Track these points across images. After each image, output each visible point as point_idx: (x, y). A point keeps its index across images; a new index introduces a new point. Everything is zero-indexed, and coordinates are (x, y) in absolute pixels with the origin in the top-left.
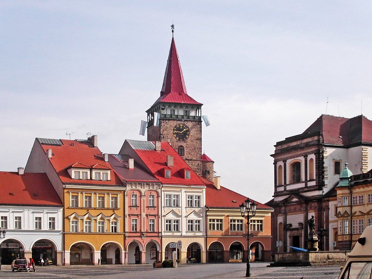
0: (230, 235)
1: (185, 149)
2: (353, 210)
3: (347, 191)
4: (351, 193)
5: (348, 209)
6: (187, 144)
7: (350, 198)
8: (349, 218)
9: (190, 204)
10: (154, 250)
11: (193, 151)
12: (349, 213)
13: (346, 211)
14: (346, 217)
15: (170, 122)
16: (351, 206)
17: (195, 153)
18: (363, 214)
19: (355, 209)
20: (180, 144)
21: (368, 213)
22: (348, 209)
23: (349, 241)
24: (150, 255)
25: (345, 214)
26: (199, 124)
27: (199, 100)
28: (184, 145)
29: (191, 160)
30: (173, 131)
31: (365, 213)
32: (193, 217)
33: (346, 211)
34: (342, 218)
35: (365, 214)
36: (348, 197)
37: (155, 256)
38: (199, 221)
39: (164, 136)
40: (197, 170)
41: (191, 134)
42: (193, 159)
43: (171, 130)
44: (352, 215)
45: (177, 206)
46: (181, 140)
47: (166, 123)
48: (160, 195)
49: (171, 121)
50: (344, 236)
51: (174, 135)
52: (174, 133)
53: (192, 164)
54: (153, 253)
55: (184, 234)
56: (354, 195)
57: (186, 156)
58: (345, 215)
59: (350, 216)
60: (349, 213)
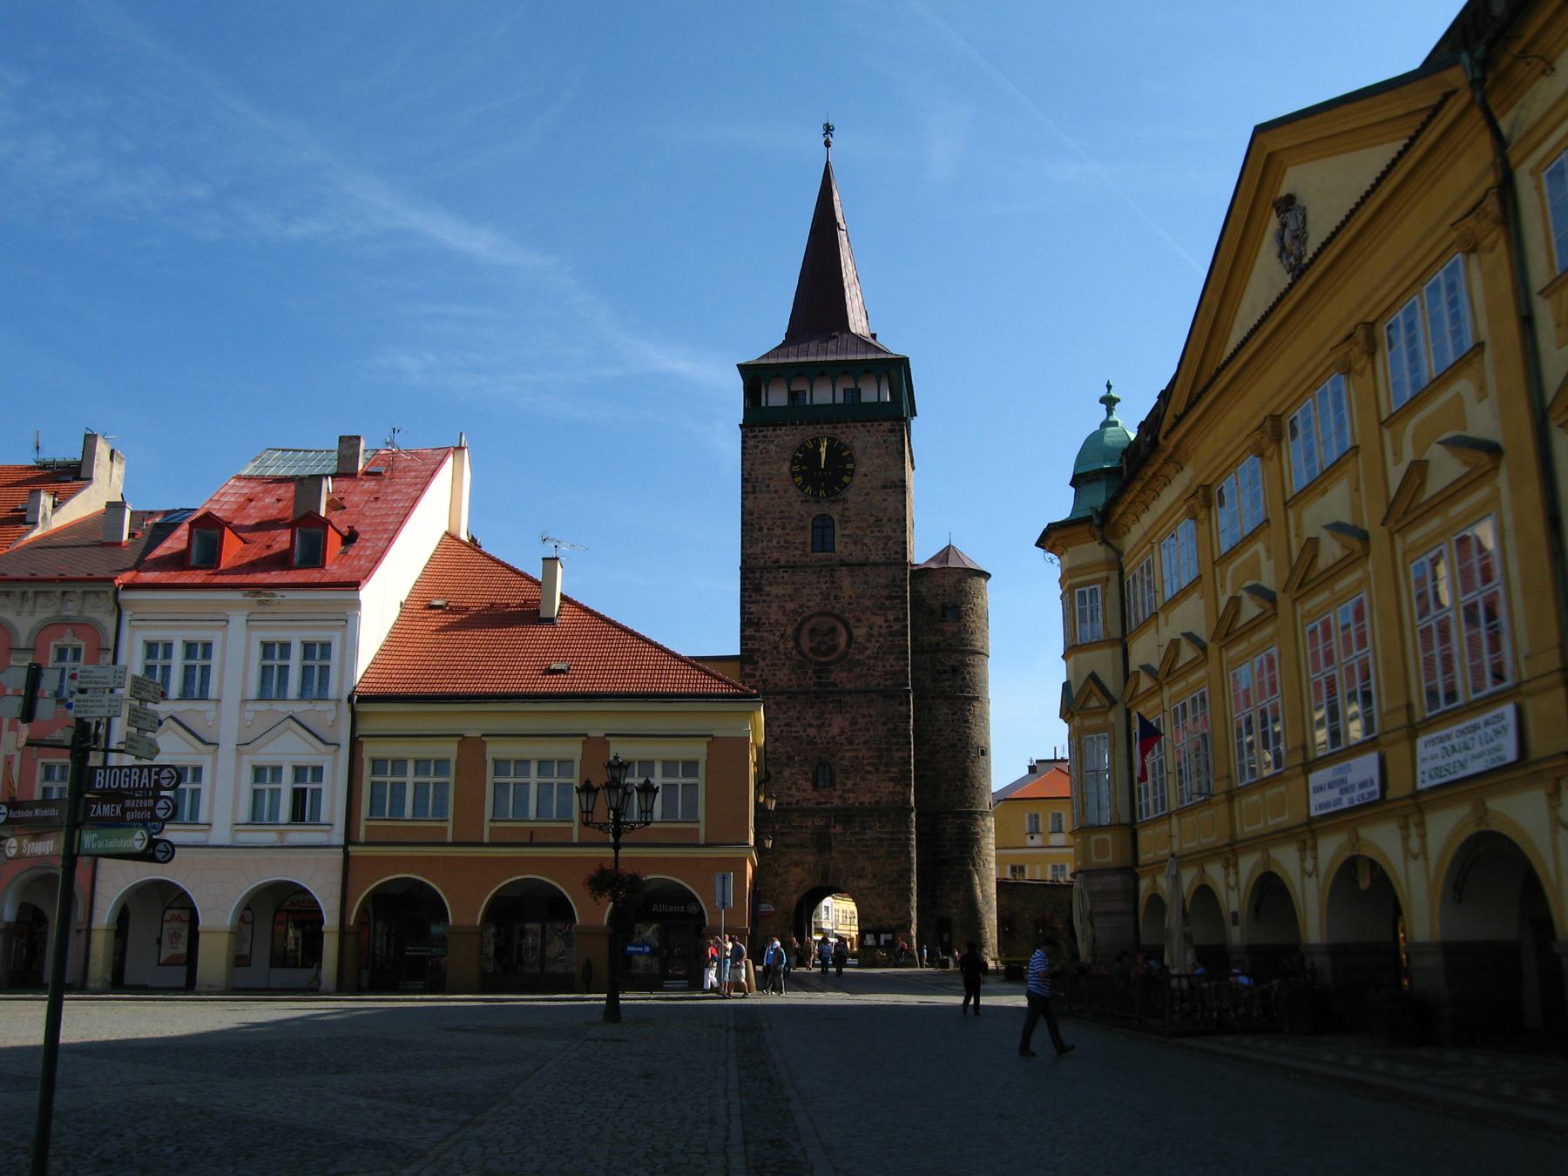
0: (486, 839)
1: (837, 526)
6: (846, 506)
8: (1111, 716)
9: (271, 683)
10: (178, 918)
11: (872, 532)
14: (1095, 712)
15: (778, 432)
17: (877, 537)
20: (816, 510)
23: (1121, 870)
24: (159, 941)
26: (892, 431)
27: (893, 345)
28: (835, 512)
29: (862, 565)
30: (793, 463)
32: (290, 749)
33: (1093, 677)
36: (1099, 587)
37: (182, 949)
38: (318, 772)
39: (754, 487)
40: (887, 603)
41: (863, 470)
42: (870, 560)
43: (784, 460)
45: (203, 696)
46: (822, 493)
47: (764, 437)
48: (111, 645)
49: (784, 428)
50: (1094, 838)
51: (797, 480)
52: (793, 475)
53: (867, 583)
54: (175, 936)
55: (221, 834)
57: (843, 548)
58: (1088, 698)
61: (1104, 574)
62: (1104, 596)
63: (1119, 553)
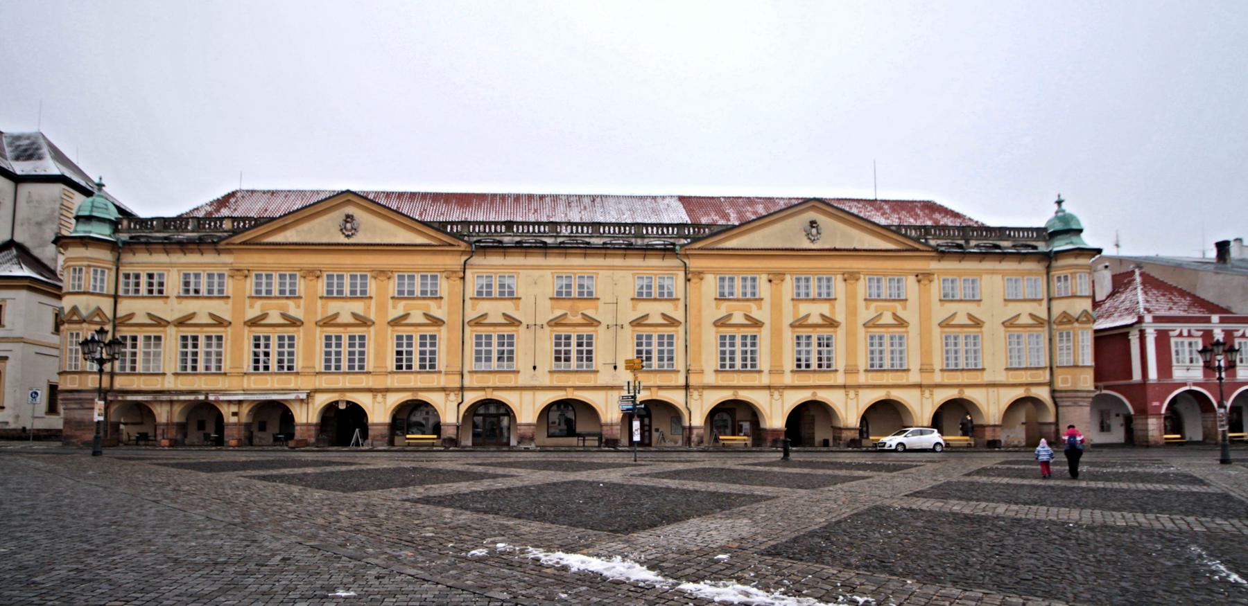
2: (119, 306)
3: (106, 255)
4: (118, 263)
5: (106, 305)
7: (113, 274)
12: (109, 314)
13: (99, 309)
16: (116, 297)
18: (160, 322)
19: (125, 307)
21: (181, 323)
22: (106, 305)
25: (74, 314)
31: (169, 319)
34: (85, 325)
35: (169, 323)
44: (117, 322)
56: (123, 270)
59: (111, 324)
60: (109, 313)
61: (110, 266)
62: (109, 275)
63: (118, 259)
